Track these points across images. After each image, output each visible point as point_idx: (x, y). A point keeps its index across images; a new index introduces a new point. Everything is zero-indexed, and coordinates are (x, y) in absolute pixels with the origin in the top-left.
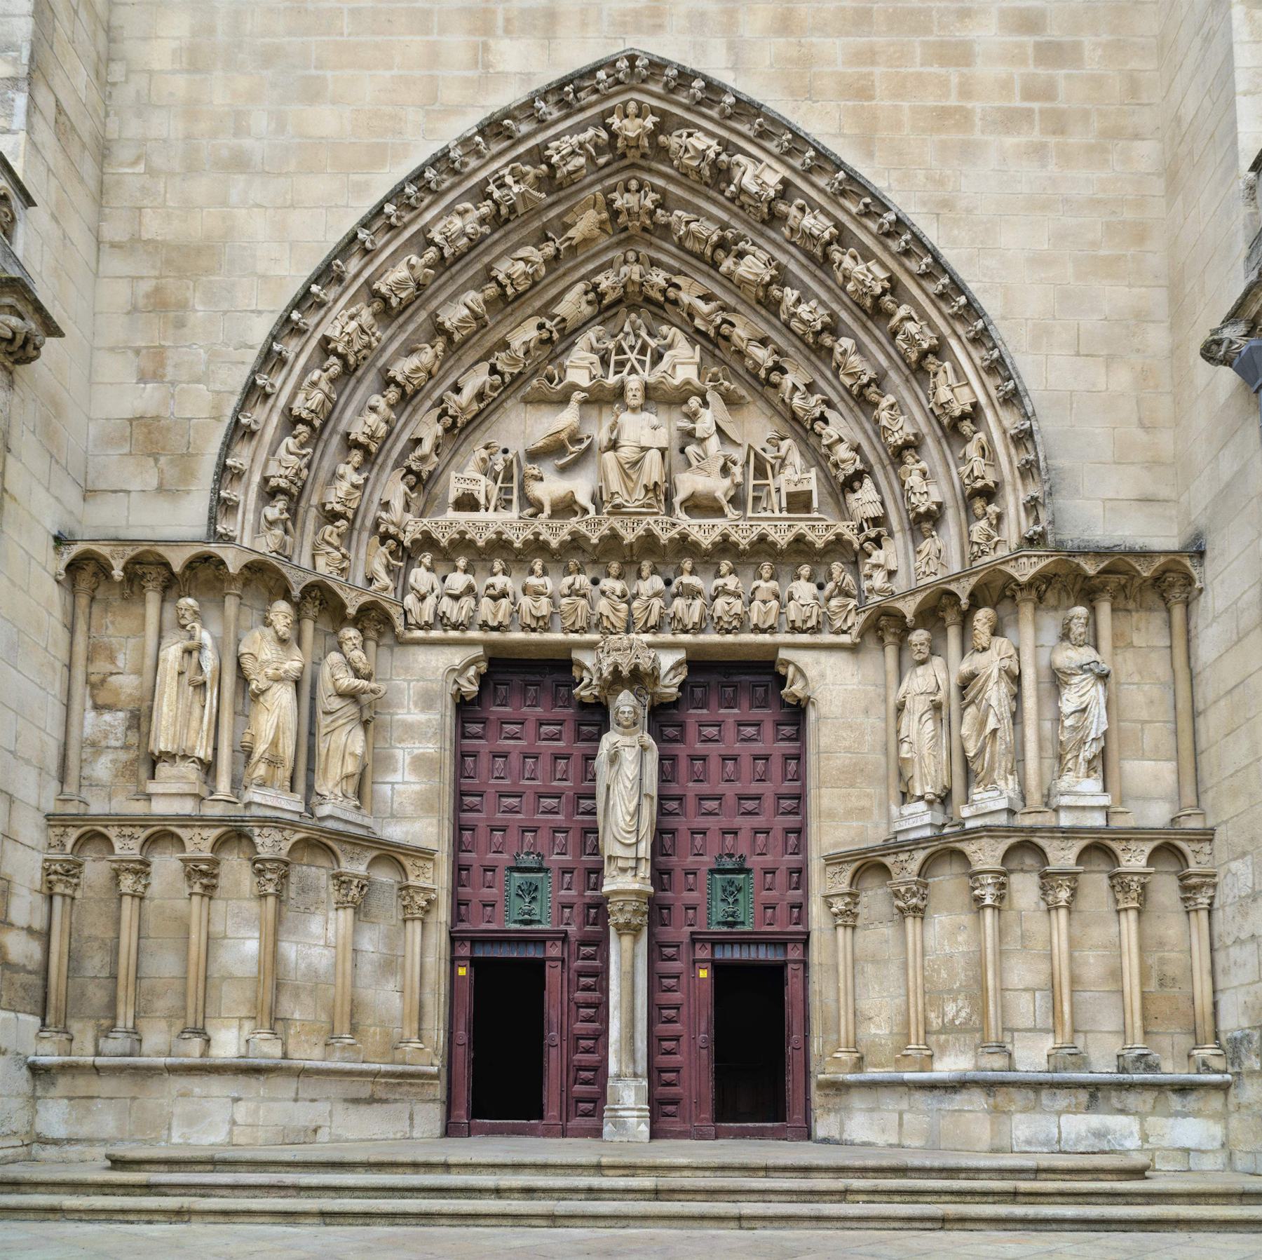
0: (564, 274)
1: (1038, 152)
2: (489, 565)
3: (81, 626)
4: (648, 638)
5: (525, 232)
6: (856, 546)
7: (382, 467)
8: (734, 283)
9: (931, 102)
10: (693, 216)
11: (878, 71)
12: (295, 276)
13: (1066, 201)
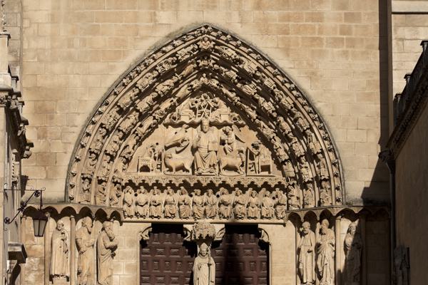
1: (345, 54)
4: (211, 220)
10: (226, 70)
11: (291, 23)
13: (354, 72)
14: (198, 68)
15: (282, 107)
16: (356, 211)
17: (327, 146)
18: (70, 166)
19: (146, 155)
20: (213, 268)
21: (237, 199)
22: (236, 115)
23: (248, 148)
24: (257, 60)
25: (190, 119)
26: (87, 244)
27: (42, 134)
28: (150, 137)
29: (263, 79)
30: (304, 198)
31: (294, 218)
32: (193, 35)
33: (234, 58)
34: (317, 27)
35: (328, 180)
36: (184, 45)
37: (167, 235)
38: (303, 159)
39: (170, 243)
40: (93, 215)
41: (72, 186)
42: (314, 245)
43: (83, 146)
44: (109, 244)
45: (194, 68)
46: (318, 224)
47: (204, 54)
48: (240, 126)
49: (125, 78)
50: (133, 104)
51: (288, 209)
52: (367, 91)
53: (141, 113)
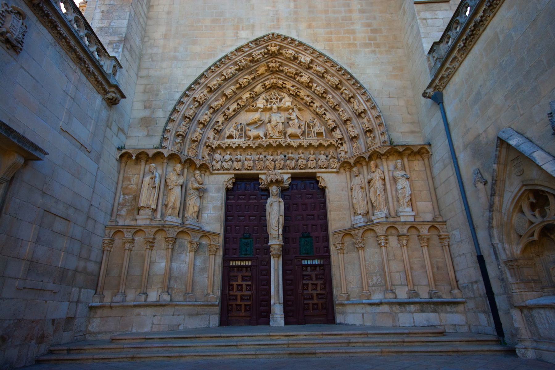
0: (257, 82)
1: (374, 52)
2: (236, 153)
3: (122, 172)
4: (280, 171)
5: (246, 72)
6: (336, 146)
7: (208, 129)
8: (301, 83)
9: (346, 42)
10: (289, 68)
11: (333, 36)
12: (187, 83)
13: (382, 63)
20: (282, 204)
44: (196, 185)
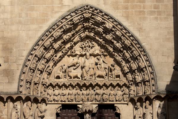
1: (156, 18)
4: (91, 103)
6: (128, 85)
10: (98, 28)
11: (129, 4)
13: (161, 28)
14: (84, 27)
15: (125, 45)
16: (163, 96)
17: (148, 64)
18: (20, 76)
19: (59, 70)
21: (104, 92)
22: (103, 50)
23: (109, 67)
24: (112, 22)
25: (80, 52)
26: (29, 115)
27: (6, 61)
28: (61, 62)
29: (116, 32)
30: (137, 90)
31: (132, 101)
32: (81, 10)
33: (101, 21)
34: (142, 6)
35: (148, 81)
36: (76, 16)
37: (70, 110)
38: (136, 71)
39: (71, 114)
40: (32, 100)
41: (21, 86)
42: (142, 114)
43: (26, 66)
44: (40, 115)
45: (82, 27)
46: (144, 103)
47: (87, 20)
48: (105, 56)
49: (47, 32)
50: (51, 45)
51: (129, 96)
52: (167, 37)
53: (55, 50)
